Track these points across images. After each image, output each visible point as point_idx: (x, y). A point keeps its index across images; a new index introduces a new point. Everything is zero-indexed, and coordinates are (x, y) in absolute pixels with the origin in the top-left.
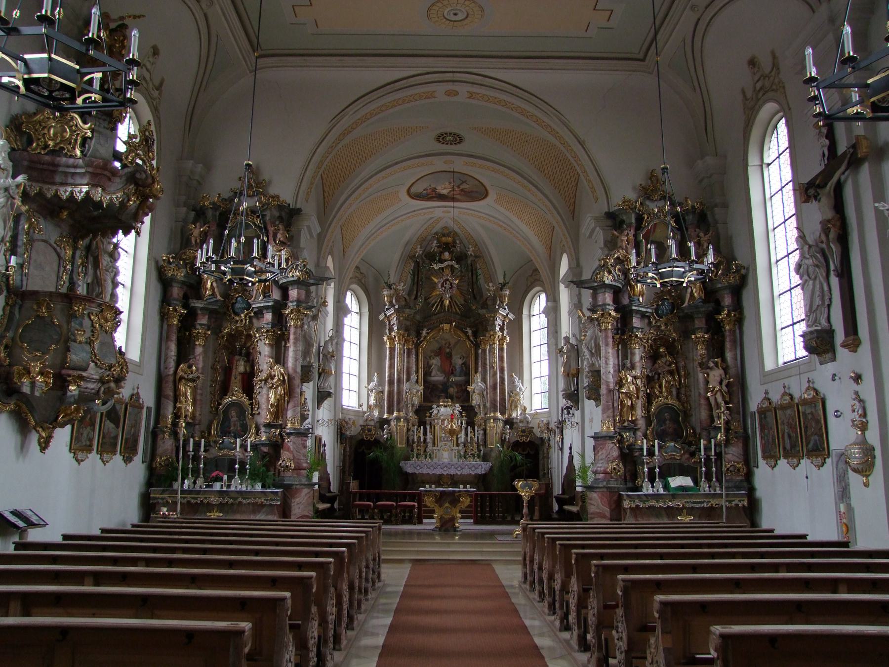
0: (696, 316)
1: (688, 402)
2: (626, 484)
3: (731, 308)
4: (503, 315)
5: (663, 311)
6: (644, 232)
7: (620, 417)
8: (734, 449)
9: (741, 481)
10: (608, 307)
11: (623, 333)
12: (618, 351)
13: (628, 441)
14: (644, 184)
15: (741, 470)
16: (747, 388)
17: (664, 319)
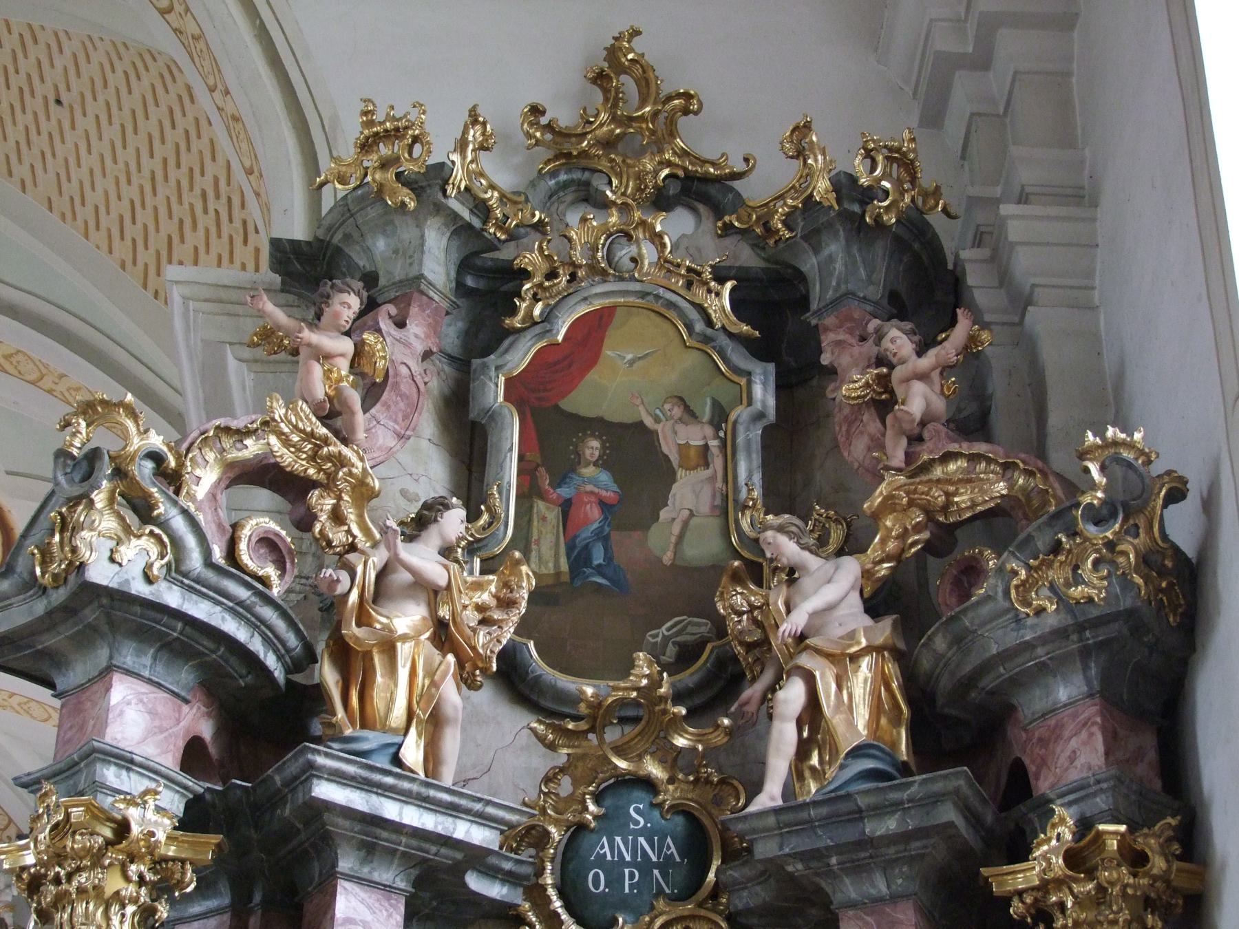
0: (849, 889)
3: (1101, 803)
5: (614, 871)
10: (111, 775)
14: (563, 115)
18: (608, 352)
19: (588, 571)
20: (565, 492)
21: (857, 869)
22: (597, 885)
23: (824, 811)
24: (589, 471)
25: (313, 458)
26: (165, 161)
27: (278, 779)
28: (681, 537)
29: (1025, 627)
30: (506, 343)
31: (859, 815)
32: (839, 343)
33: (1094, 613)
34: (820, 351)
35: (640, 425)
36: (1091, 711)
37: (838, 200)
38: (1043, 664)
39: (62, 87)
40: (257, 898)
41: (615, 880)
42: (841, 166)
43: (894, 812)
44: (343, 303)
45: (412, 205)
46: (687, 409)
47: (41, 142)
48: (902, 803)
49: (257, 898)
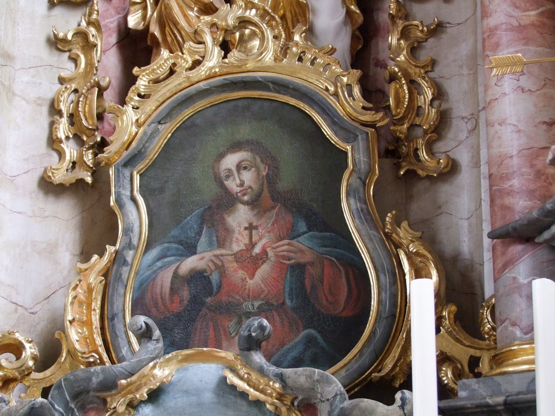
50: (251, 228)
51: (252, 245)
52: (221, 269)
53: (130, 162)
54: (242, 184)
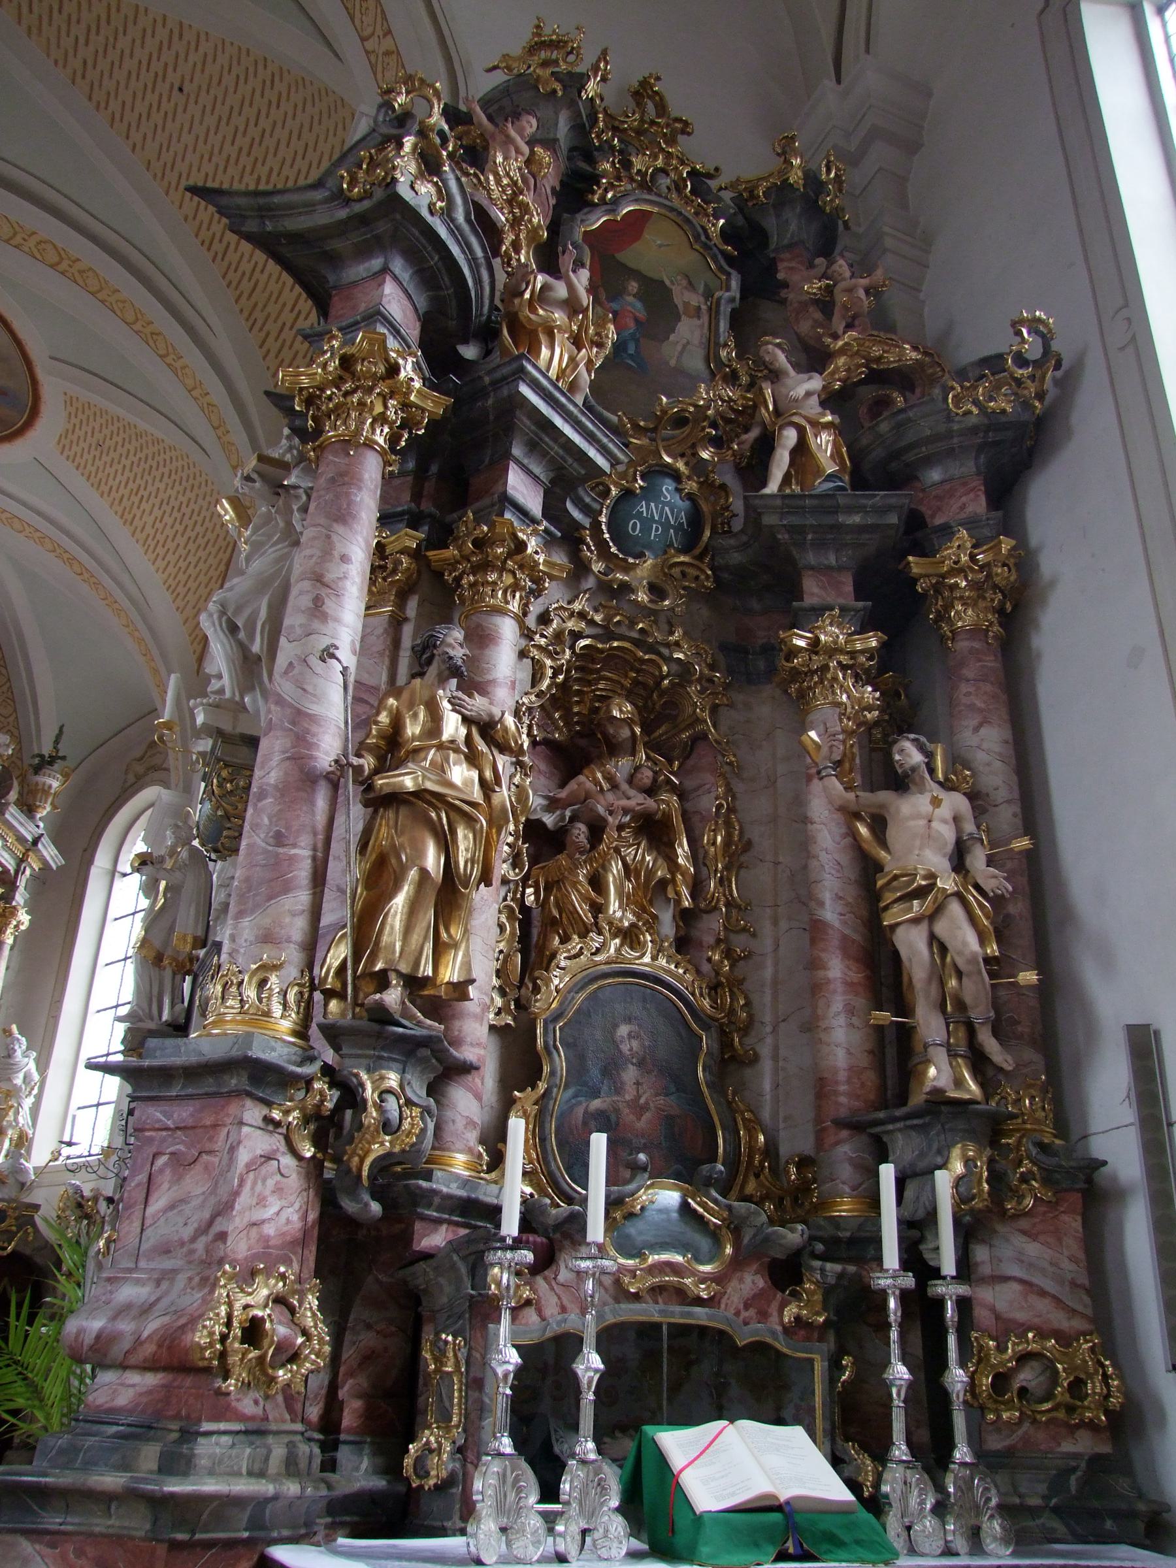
0: (811, 558)
1: (736, 984)
2: (330, 1465)
4: (21, 839)
5: (647, 523)
6: (598, 221)
7: (357, 954)
8: (1033, 1249)
9: (1096, 1461)
11: (442, 536)
12: (397, 622)
13: (386, 1126)
15: (1094, 1387)
16: (1068, 916)
17: (646, 567)
18: (647, 235)
19: (625, 355)
20: (615, 306)
21: (820, 545)
22: (634, 529)
23: (815, 502)
24: (630, 299)
25: (510, 202)
26: (241, 149)
27: (487, 380)
28: (681, 353)
29: (953, 421)
30: (586, 210)
31: (835, 510)
32: (791, 269)
33: (1003, 419)
34: (776, 271)
35: (663, 282)
36: (977, 483)
37: (804, 186)
38: (953, 449)
39: (188, 78)
40: (434, 469)
41: (646, 529)
42: (813, 166)
43: (858, 512)
44: (528, 122)
45: (560, 93)
46: (690, 283)
47: (157, 118)
48: (865, 507)
49: (434, 469)
50: (637, 1084)
51: (639, 1097)
52: (617, 1111)
53: (556, 1018)
54: (631, 1050)
